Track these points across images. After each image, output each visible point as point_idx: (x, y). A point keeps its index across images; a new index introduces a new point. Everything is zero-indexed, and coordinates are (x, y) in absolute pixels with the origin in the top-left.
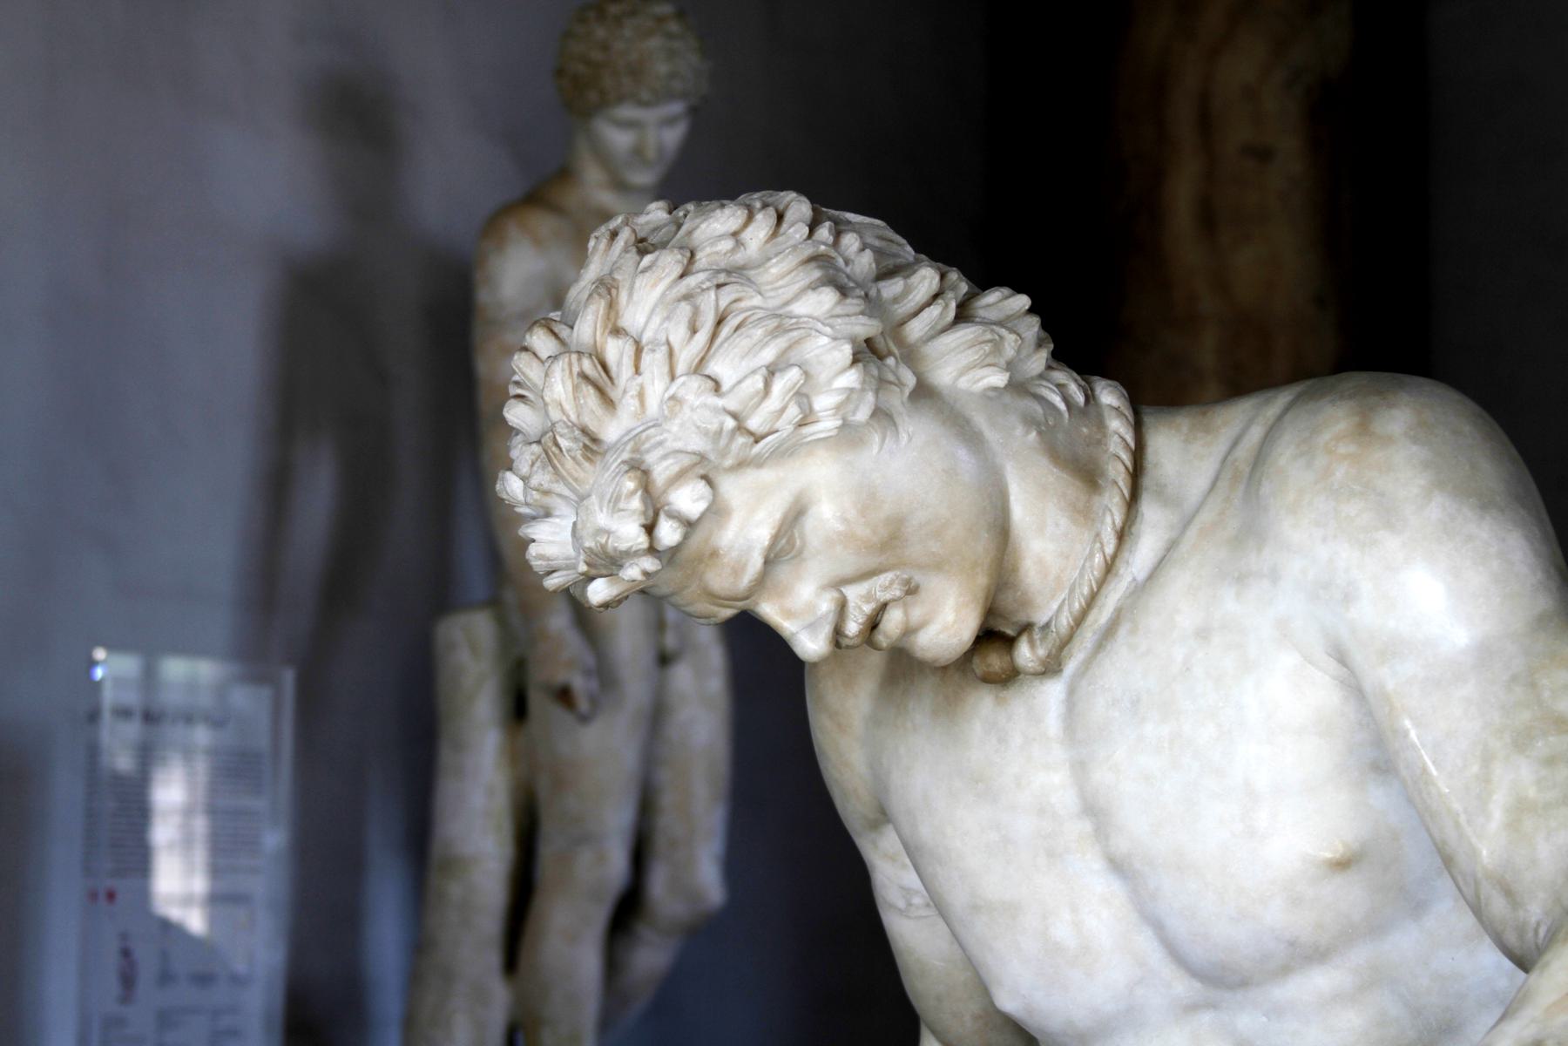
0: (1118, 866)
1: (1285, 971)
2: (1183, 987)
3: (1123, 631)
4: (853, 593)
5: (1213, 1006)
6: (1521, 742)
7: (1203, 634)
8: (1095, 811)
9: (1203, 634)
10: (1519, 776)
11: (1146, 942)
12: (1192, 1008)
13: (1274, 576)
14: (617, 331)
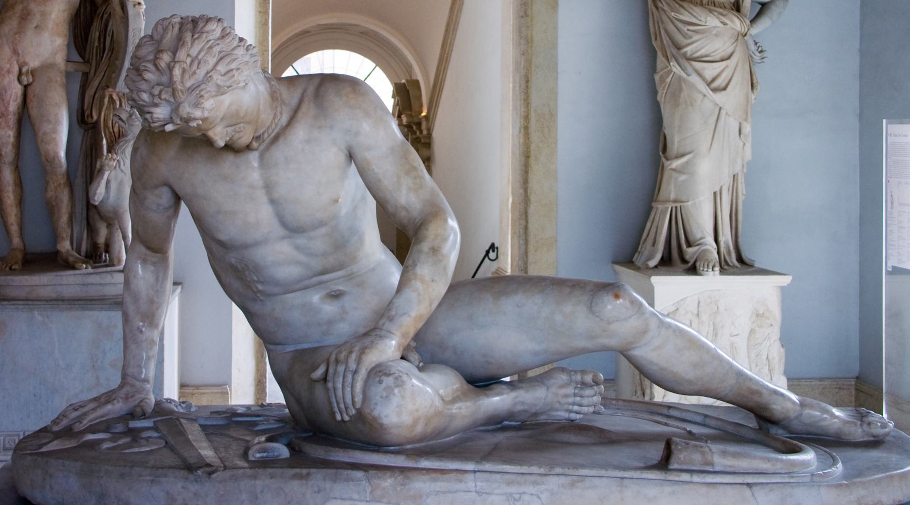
0: (273, 202)
1: (317, 228)
2: (281, 231)
3: (281, 140)
4: (229, 129)
5: (289, 237)
6: (407, 173)
7: (308, 141)
8: (269, 187)
9: (308, 141)
10: (407, 182)
11: (275, 223)
12: (284, 238)
13: (331, 128)
14: (188, 55)
